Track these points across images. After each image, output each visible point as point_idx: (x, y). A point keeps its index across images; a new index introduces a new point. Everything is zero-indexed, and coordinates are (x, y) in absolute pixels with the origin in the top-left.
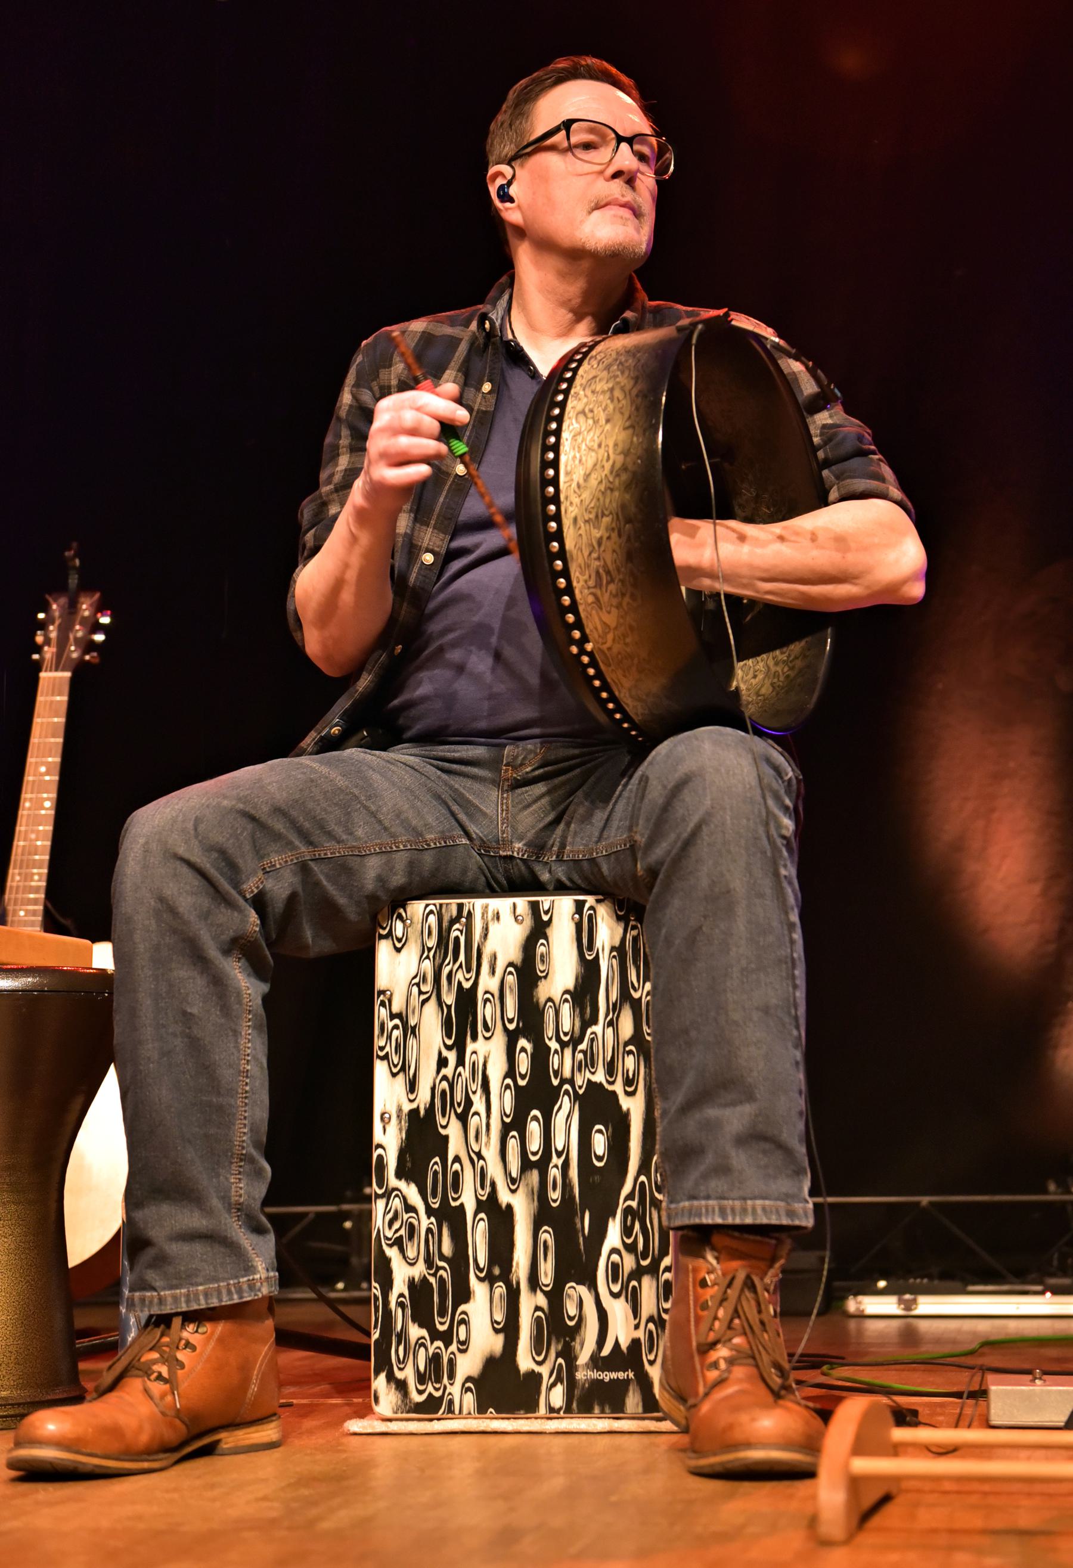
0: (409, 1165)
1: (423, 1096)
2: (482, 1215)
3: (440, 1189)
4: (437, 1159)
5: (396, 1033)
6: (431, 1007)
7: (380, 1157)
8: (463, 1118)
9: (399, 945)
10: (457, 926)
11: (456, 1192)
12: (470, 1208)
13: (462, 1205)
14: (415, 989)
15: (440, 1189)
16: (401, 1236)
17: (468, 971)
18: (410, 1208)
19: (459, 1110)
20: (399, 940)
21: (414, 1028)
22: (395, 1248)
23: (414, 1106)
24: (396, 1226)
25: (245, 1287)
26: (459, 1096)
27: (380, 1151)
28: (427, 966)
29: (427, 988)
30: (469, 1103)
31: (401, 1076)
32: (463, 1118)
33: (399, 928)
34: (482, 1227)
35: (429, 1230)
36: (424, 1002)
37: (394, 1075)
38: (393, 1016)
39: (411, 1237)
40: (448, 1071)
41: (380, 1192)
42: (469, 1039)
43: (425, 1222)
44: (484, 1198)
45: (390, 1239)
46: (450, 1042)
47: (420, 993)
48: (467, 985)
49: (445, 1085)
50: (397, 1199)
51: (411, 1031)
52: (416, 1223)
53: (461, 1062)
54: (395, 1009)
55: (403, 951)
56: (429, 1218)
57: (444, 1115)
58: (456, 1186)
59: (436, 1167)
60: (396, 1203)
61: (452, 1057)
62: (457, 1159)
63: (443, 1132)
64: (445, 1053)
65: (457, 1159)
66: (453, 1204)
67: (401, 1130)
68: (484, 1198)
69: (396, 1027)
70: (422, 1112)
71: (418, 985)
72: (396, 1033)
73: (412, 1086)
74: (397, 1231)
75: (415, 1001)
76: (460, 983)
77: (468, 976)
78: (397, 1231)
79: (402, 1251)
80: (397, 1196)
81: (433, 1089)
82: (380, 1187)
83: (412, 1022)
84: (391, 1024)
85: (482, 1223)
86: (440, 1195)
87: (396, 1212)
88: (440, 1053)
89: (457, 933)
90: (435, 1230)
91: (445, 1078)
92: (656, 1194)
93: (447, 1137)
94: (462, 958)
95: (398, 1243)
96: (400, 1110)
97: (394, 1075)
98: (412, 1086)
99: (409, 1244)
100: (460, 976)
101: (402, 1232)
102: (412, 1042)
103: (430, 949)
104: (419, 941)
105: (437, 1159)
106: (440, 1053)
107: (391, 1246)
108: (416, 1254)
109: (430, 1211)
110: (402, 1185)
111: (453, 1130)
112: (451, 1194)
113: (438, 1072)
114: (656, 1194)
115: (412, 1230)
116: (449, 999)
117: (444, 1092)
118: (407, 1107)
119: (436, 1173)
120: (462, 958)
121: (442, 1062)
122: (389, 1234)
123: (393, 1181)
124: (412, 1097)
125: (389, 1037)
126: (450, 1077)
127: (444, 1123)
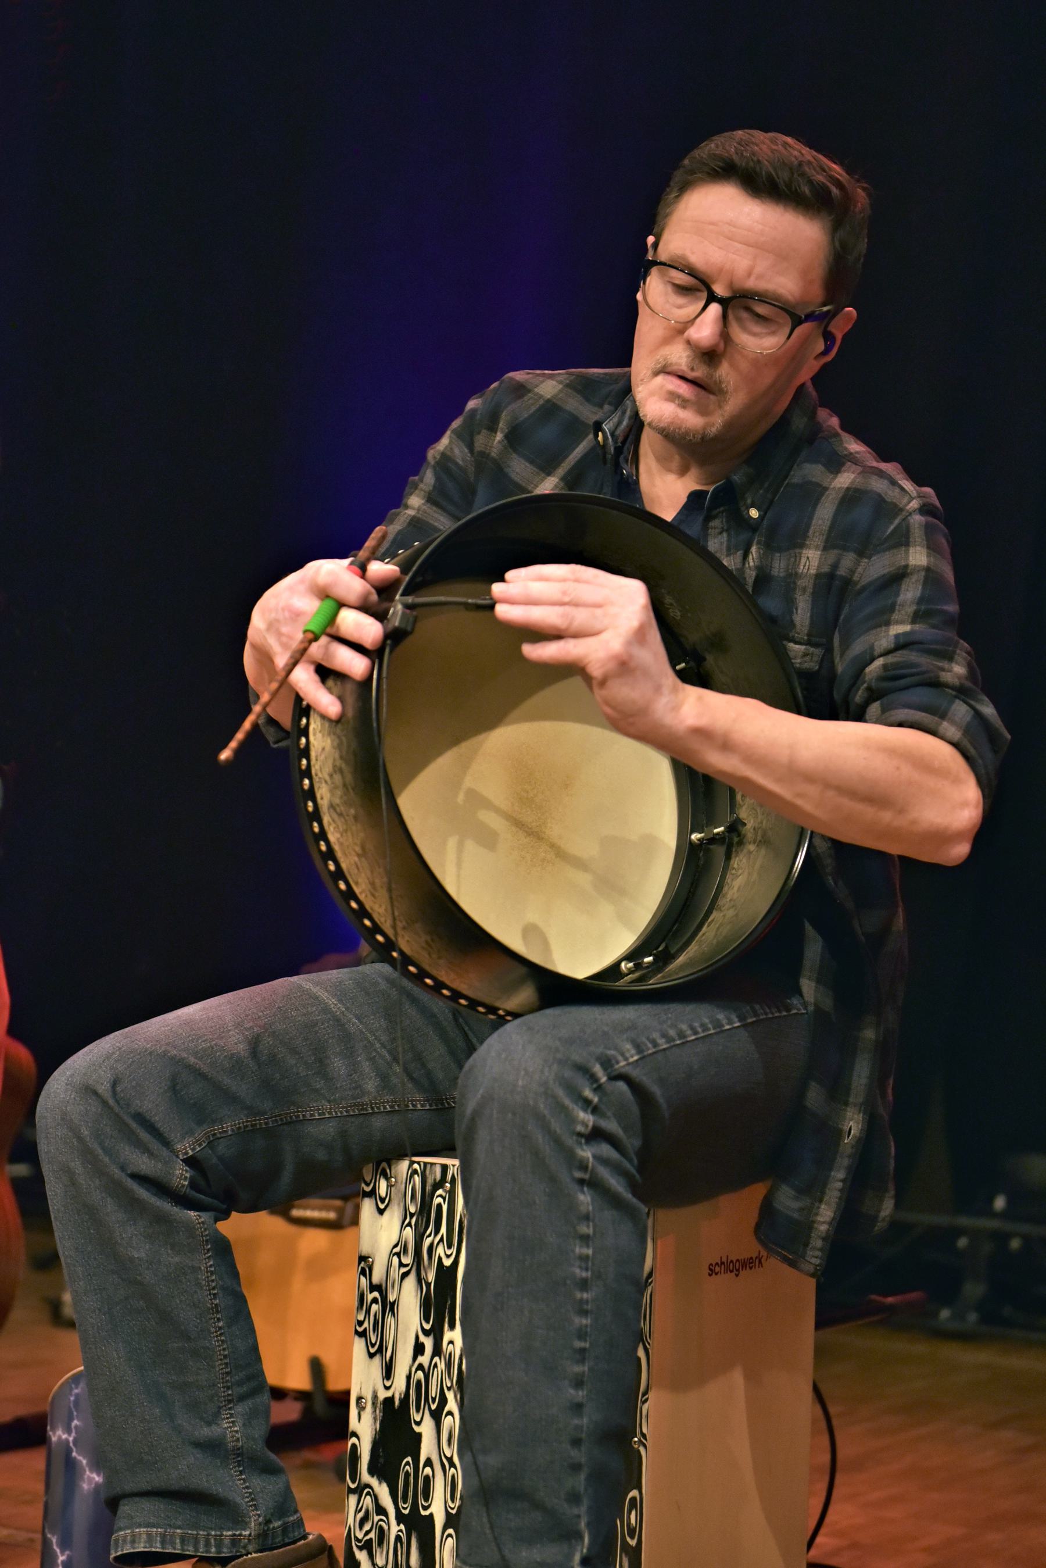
0: (382, 1460)
1: (399, 1384)
2: (451, 1531)
3: (410, 1494)
4: (409, 1459)
5: (375, 1307)
6: (410, 1282)
7: (354, 1446)
8: (437, 1416)
9: (382, 1206)
10: (440, 1192)
11: (426, 1500)
12: (439, 1521)
13: (431, 1515)
14: (395, 1260)
15: (410, 1494)
16: (371, 1539)
17: (449, 1247)
18: (381, 1510)
19: (433, 1407)
20: (383, 1200)
21: (392, 1304)
22: (365, 1553)
23: (389, 1394)
24: (367, 1527)
25: (227, 1541)
26: (434, 1391)
27: (354, 1440)
28: (409, 1232)
29: (407, 1260)
30: (443, 1401)
31: (377, 1358)
32: (437, 1416)
33: (383, 1187)
34: (450, 1543)
35: (398, 1538)
36: (405, 1275)
37: (371, 1356)
38: (373, 1288)
39: (380, 1543)
40: (424, 1360)
41: (353, 1486)
42: (446, 1326)
43: (395, 1529)
44: (454, 1512)
45: (359, 1541)
46: (427, 1327)
47: (401, 1265)
48: (447, 1262)
49: (420, 1375)
50: (368, 1497)
51: (390, 1307)
52: (386, 1527)
53: (437, 1351)
54: (376, 1280)
55: (386, 1214)
56: (398, 1525)
57: (418, 1411)
58: (427, 1494)
59: (407, 1467)
60: (368, 1501)
61: (428, 1343)
62: (429, 1462)
63: (417, 1429)
64: (422, 1338)
65: (429, 1462)
66: (423, 1513)
67: (375, 1419)
68: (454, 1512)
69: (375, 1301)
70: (397, 1403)
71: (398, 1254)
72: (375, 1307)
73: (388, 1371)
74: (367, 1533)
75: (396, 1273)
76: (440, 1259)
77: (449, 1252)
78: (367, 1533)
79: (371, 1557)
80: (368, 1494)
81: (409, 1377)
82: (353, 1482)
83: (392, 1298)
84: (370, 1297)
85: (450, 1539)
86: (410, 1501)
87: (367, 1511)
88: (417, 1337)
89: (440, 1200)
90: (404, 1539)
91: (421, 1367)
92: (628, 1539)
93: (420, 1435)
94: (443, 1230)
95: (367, 1546)
96: (375, 1397)
97: (371, 1356)
98: (388, 1371)
99: (378, 1550)
100: (440, 1251)
101: (372, 1535)
102: (390, 1320)
103: (412, 1215)
104: (402, 1205)
105: (409, 1459)
106: (417, 1337)
107: (361, 1548)
108: (384, 1562)
109: (400, 1518)
110: (374, 1482)
111: (426, 1429)
112: (421, 1501)
113: (415, 1359)
114: (628, 1539)
115: (382, 1534)
116: (431, 1277)
117: (419, 1382)
118: (383, 1394)
119: (407, 1474)
120: (443, 1230)
121: (419, 1349)
122: (360, 1535)
123: (366, 1477)
124: (388, 1384)
125: (368, 1311)
126: (426, 1366)
127: (418, 1419)
